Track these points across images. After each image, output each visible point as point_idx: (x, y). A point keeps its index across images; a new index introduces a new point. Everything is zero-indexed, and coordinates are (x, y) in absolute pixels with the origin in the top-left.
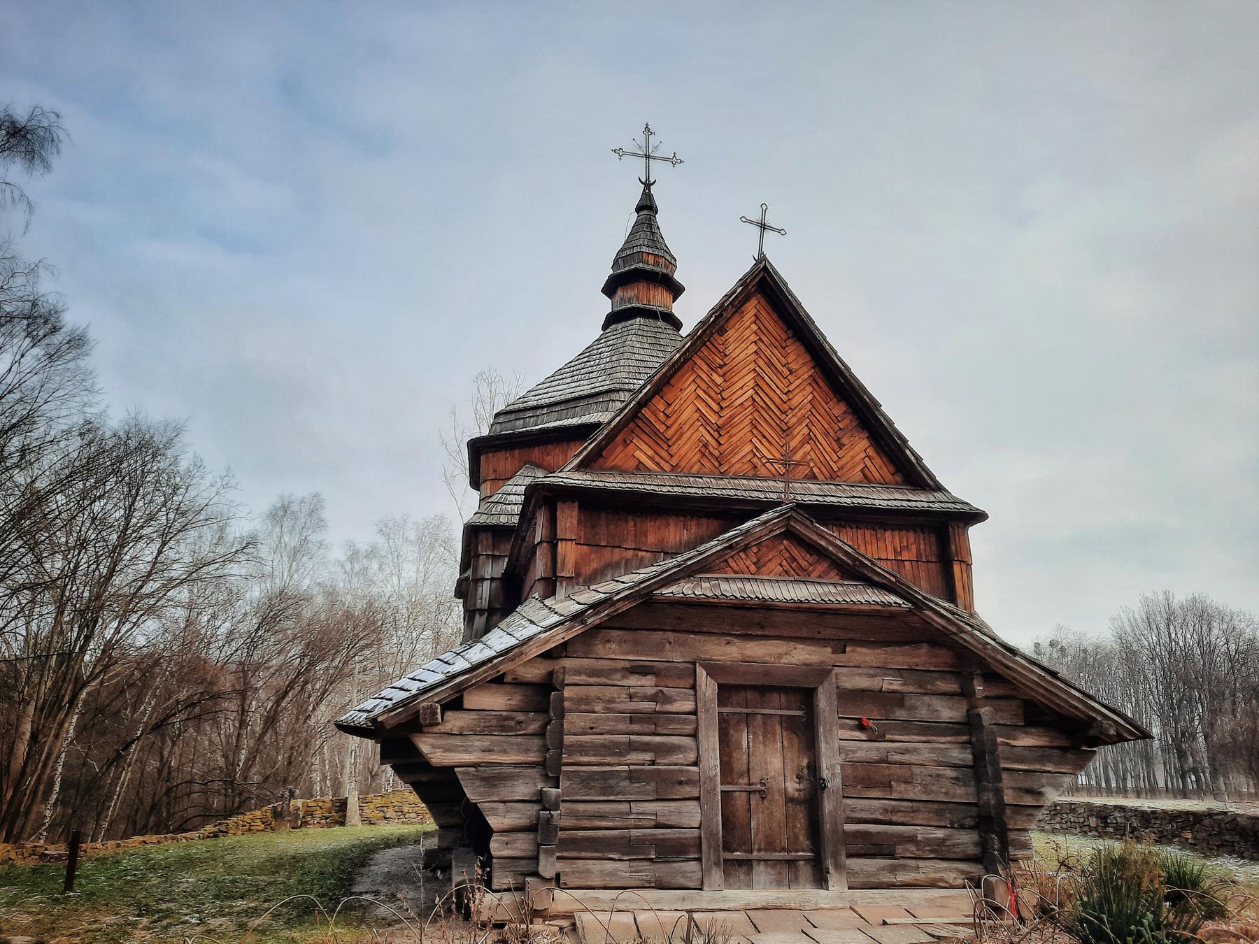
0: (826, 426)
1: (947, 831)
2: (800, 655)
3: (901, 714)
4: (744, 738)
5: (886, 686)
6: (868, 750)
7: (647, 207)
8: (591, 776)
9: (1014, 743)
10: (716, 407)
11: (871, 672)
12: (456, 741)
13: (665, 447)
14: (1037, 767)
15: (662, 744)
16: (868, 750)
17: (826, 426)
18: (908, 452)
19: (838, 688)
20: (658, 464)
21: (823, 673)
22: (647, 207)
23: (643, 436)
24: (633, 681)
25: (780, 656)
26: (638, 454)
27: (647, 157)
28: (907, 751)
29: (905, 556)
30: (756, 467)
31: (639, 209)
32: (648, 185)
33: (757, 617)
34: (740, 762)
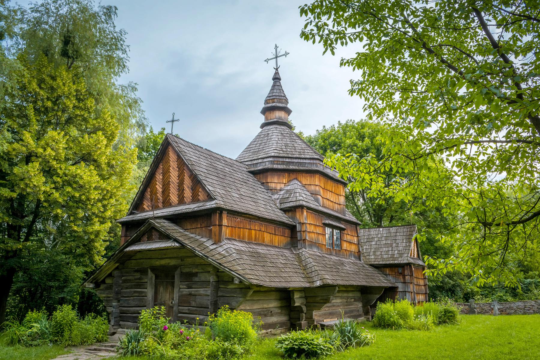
0: (188, 184)
1: (204, 316)
2: (173, 262)
3: (196, 279)
4: (161, 289)
5: (194, 271)
6: (186, 291)
7: (277, 79)
8: (126, 300)
9: (228, 287)
10: (161, 186)
11: (190, 266)
12: (102, 292)
13: (150, 202)
14: (233, 295)
15: (141, 291)
16: (186, 291)
17: (188, 184)
18: (206, 188)
19: (181, 272)
20: (149, 208)
21: (175, 267)
22: (277, 79)
23: (146, 201)
24: (136, 274)
25: (169, 263)
26: (145, 206)
27: (276, 57)
28: (197, 291)
29: (203, 225)
30: (171, 203)
31: (274, 79)
32: (277, 69)
33: (164, 251)
34: (159, 297)
